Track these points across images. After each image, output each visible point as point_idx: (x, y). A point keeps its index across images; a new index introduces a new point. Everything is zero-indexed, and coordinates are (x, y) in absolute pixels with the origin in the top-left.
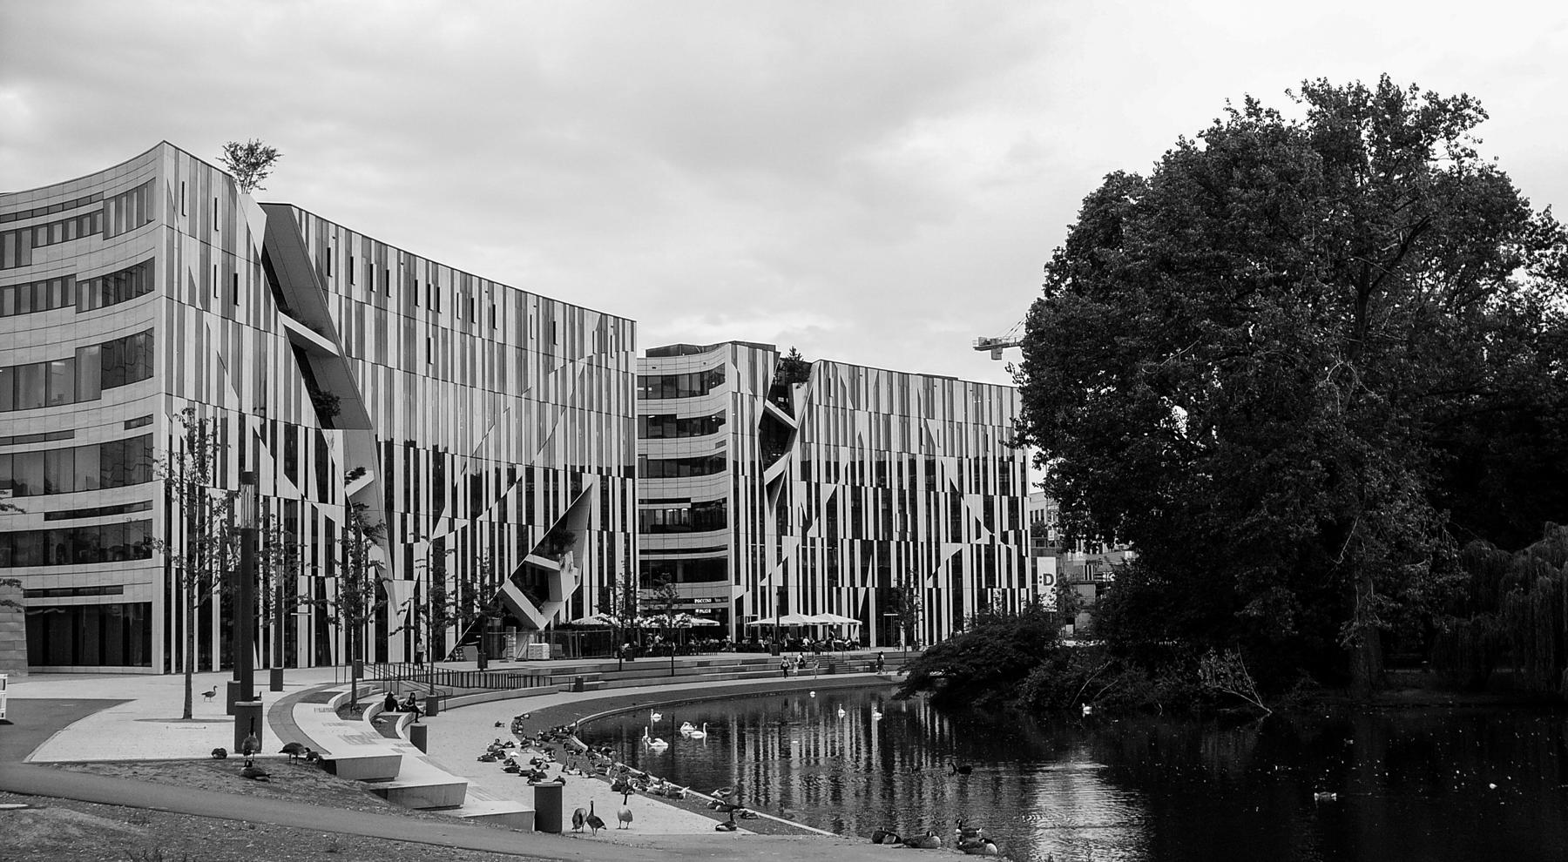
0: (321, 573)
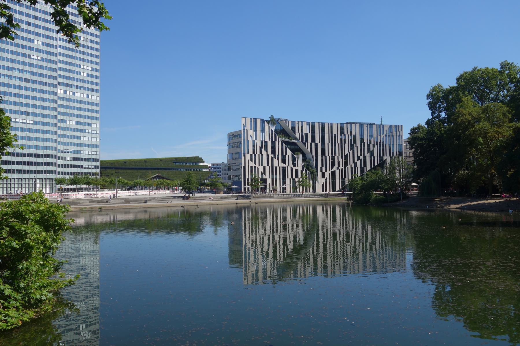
0: (294, 177)
